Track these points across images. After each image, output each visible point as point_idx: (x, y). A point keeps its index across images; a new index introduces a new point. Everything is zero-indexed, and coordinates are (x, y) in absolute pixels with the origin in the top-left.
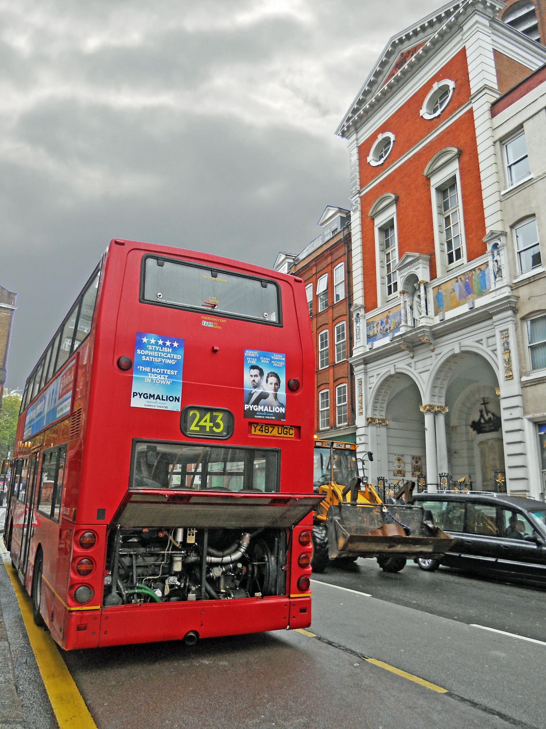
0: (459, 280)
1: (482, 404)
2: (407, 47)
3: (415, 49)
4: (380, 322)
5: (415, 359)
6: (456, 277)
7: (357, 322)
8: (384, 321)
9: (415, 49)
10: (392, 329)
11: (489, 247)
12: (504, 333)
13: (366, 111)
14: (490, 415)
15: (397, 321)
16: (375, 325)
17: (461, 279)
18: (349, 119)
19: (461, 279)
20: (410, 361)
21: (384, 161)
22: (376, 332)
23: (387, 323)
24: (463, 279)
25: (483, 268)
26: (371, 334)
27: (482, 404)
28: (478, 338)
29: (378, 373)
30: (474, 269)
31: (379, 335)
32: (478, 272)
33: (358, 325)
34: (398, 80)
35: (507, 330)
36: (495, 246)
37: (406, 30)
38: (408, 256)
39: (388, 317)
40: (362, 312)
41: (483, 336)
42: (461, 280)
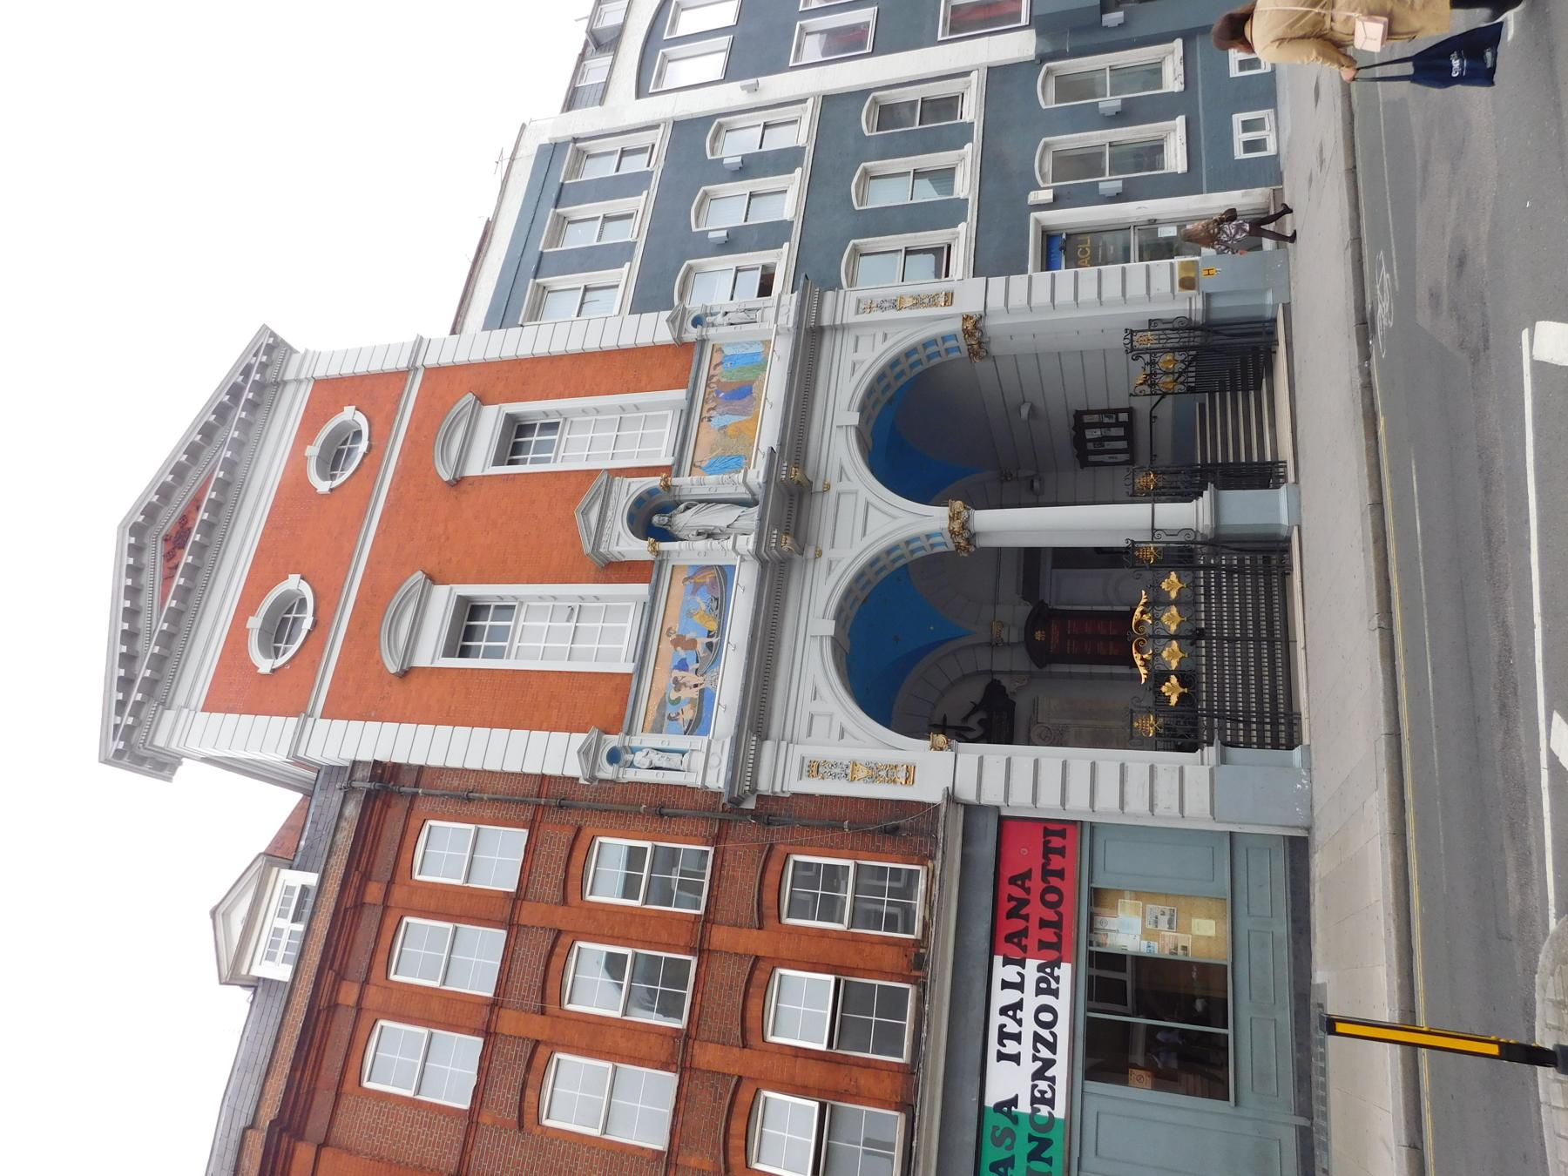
0: (713, 413)
1: (945, 719)
2: (168, 520)
3: (196, 504)
4: (677, 673)
5: (825, 545)
6: (701, 420)
7: (632, 765)
8: (682, 653)
9: (196, 504)
10: (714, 626)
11: (692, 334)
13: (159, 662)
14: (973, 722)
15: (703, 607)
16: (674, 695)
18: (121, 705)
20: (823, 563)
21: (315, 614)
22: (694, 694)
24: (712, 405)
26: (689, 714)
27: (945, 719)
29: (809, 694)
32: (720, 369)
33: (639, 758)
34: (192, 571)
35: (859, 301)
36: (697, 322)
37: (118, 566)
38: (585, 513)
39: (679, 642)
40: (613, 741)
41: (848, 356)
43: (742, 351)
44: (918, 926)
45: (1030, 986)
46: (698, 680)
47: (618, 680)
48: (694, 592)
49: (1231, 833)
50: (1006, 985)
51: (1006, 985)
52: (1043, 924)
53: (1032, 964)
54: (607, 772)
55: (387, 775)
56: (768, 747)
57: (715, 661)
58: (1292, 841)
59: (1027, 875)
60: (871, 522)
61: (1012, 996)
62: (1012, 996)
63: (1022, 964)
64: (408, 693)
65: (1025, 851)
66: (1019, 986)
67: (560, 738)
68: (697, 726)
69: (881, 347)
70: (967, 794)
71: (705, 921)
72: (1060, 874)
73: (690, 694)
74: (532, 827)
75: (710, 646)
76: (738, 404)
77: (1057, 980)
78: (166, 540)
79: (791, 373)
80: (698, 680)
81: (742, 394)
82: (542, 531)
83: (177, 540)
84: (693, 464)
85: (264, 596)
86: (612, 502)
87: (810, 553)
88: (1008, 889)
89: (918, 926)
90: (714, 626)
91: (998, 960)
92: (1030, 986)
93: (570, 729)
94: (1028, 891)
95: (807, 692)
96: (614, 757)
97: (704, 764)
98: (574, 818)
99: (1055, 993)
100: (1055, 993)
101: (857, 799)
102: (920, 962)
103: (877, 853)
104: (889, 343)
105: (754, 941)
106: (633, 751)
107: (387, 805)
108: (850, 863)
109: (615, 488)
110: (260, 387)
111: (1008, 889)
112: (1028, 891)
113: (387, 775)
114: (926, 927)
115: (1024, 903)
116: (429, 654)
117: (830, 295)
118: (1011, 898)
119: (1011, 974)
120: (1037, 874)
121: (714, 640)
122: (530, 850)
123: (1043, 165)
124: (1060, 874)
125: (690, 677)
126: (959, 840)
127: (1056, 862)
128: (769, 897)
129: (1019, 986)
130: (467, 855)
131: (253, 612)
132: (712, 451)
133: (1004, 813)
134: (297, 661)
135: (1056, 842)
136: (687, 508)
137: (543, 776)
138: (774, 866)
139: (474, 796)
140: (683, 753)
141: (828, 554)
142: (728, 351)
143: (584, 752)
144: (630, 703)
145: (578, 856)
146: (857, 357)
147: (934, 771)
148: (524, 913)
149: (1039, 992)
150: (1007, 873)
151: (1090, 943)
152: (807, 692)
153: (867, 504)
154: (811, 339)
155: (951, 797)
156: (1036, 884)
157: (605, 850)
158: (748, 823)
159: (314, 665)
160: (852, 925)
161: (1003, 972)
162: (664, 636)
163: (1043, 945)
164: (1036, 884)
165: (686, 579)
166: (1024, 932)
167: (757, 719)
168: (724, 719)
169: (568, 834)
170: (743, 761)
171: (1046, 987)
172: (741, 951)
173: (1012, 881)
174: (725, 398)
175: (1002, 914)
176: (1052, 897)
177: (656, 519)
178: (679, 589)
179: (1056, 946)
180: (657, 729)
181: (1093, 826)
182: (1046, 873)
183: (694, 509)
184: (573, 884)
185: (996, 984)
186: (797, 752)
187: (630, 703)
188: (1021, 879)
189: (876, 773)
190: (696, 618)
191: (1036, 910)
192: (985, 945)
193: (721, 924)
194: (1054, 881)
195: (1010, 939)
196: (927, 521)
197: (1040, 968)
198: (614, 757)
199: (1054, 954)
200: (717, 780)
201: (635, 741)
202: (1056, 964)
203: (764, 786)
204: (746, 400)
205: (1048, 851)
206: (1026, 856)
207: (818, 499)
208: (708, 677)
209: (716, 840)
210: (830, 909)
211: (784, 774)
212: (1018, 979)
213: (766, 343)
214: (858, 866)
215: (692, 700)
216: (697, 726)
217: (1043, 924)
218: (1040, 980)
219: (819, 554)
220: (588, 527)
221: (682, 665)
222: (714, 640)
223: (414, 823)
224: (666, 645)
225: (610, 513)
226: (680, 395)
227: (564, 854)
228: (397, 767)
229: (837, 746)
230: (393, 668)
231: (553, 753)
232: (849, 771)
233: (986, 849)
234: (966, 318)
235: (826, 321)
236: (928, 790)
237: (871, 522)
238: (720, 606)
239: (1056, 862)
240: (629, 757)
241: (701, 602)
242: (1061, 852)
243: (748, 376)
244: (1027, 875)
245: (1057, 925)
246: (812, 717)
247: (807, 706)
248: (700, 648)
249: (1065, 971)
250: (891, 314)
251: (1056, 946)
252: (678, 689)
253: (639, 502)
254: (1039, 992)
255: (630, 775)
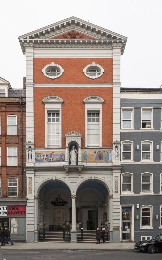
0: (96, 153)
2: (78, 30)
4: (46, 155)
5: (69, 176)
6: (95, 151)
7: (29, 150)
10: (54, 160)
12: (117, 177)
17: (97, 152)
19: (97, 152)
20: (66, 176)
21: (55, 78)
22: (42, 159)
23: (51, 157)
24: (98, 153)
25: (108, 152)
26: (39, 158)
28: (103, 176)
30: (104, 151)
31: (44, 160)
33: (30, 151)
35: (118, 177)
38: (73, 133)
39: (51, 154)
40: (33, 147)
41: (106, 176)
42: (97, 153)
43: (110, 156)
44: (9, 196)
45: (3, 211)
46: (45, 159)
47: (44, 145)
48: (60, 156)
49: (26, 234)
50: (3, 208)
51: (3, 208)
52: (12, 212)
53: (6, 211)
54: (27, 147)
55: (24, 105)
56: (33, 172)
57: (48, 161)
58: (26, 241)
59: (18, 210)
60: (73, 183)
61: (2, 209)
62: (2, 209)
63: (6, 210)
64: (39, 104)
65: (21, 209)
66: (3, 210)
67: (33, 137)
68: (37, 160)
69: (108, 182)
70: (28, 201)
71: (6, 167)
72: (19, 214)
73: (42, 158)
74: (18, 135)
75: (51, 160)
76: (98, 157)
77: (5, 214)
78: (73, 31)
79: (101, 167)
80: (45, 159)
81: (100, 157)
82: (73, 123)
83: (73, 35)
84: (86, 151)
85: (59, 64)
86: (76, 138)
87: (67, 174)
88: (16, 207)
89: (9, 196)
90: (54, 160)
91: (6, 207)
92: (3, 211)
93: (34, 139)
94: (16, 210)
95: (43, 177)
96: (30, 147)
97: (30, 163)
98: (20, 142)
99: (3, 214)
100: (3, 214)
101: (26, 186)
102: (4, 197)
103: (19, 190)
104: (109, 183)
105: (4, 174)
106: (31, 150)
107: (19, 107)
108: (17, 186)
109: (78, 138)
110: (110, 43)
111: (16, 207)
112: (16, 210)
113: (24, 105)
114: (9, 197)
115: (14, 209)
116: (48, 107)
117: (120, 171)
118: (15, 208)
119: (5, 208)
120: (19, 211)
121: (52, 160)
122: (13, 136)
123: (146, 206)
124: (19, 214)
125: (45, 157)
126: (21, 201)
127: (20, 213)
128: (11, 175)
129: (3, 210)
130: (12, 125)
131: (55, 63)
132: (88, 154)
133: (26, 206)
134: (45, 78)
135: (23, 213)
136: (76, 152)
137: (26, 135)
138: (15, 175)
139: (22, 123)
140: (31, 159)
141: (67, 177)
142: (110, 154)
143: (30, 142)
144: (41, 148)
145: (14, 144)
146: (106, 178)
147: (31, 196)
148: (3, 137)
149: (3, 212)
150: (18, 207)
151: (10, 218)
152: (43, 177)
153: (76, 182)
154: (110, 169)
155: (27, 199)
156: (17, 211)
157: (15, 149)
158: (21, 170)
159: (45, 82)
160: (9, 187)
161: (5, 208)
162: (52, 152)
163: (9, 212)
164: (17, 211)
165: (63, 154)
166: (10, 210)
167: (37, 170)
168: (38, 165)
169: (17, 142)
170: (30, 169)
171: (3, 213)
172: (3, 172)
173: (17, 208)
174: (99, 155)
175: (13, 207)
176: (15, 213)
177: (73, 146)
178: (61, 153)
179: (9, 214)
180: (36, 154)
181: (26, 217)
182: (19, 212)
183: (75, 153)
184: (9, 145)
185: (3, 207)
186: (33, 177)
187: (41, 148)
188: (17, 209)
189: (31, 188)
190: (55, 157)
191: (14, 211)
192: (8, 205)
193: (6, 169)
194: (18, 213)
195: (9, 208)
196: (74, 193)
197: (6, 212)
198: (30, 147)
199: (8, 214)
200: (27, 165)
201: (33, 150)
202: (7, 214)
203: (27, 172)
204: (99, 159)
205: (22, 212)
206: (21, 209)
207: (77, 174)
208: (45, 161)
209: (18, 166)
210: (10, 184)
211: (29, 175)
212: (4, 209)
213: (111, 161)
214: (17, 187)
215: (41, 159)
216: (37, 160)
217: (12, 212)
218: (4, 212)
219: (67, 176)
220: (71, 134)
221: (47, 156)
222: (52, 160)
223: (16, 113)
224: (51, 152)
225: (73, 138)
226: (101, 146)
227: (14, 142)
228: (25, 107)
229: (35, 183)
230: (43, 101)
231: (30, 137)
232: (31, 184)
233: (21, 204)
234: (112, 195)
235: (114, 171)
236: (28, 196)
237: (73, 183)
238: (57, 161)
239: (20, 213)
240: (30, 150)
241: (59, 157)
242: (22, 214)
243: (104, 158)
244: (18, 210)
245: (12, 214)
246: (39, 178)
247: (41, 177)
248: (50, 158)
249: (6, 215)
250: (114, 183)
251: (9, 214)
252: (43, 156)
253: (76, 143)
254: (3, 212)
255: (27, 151)
